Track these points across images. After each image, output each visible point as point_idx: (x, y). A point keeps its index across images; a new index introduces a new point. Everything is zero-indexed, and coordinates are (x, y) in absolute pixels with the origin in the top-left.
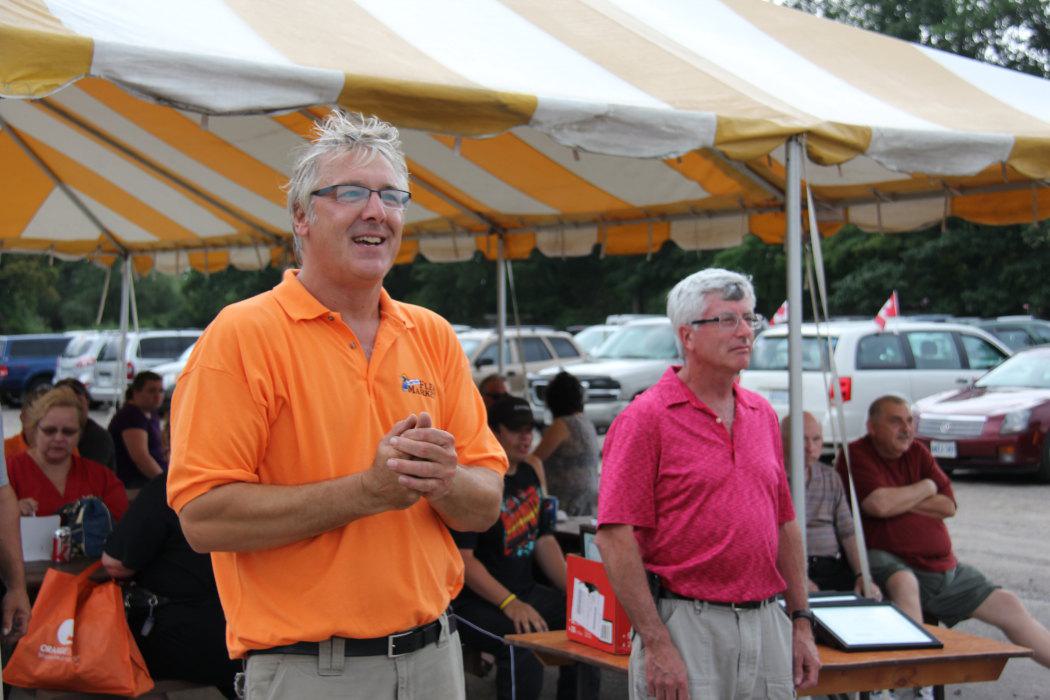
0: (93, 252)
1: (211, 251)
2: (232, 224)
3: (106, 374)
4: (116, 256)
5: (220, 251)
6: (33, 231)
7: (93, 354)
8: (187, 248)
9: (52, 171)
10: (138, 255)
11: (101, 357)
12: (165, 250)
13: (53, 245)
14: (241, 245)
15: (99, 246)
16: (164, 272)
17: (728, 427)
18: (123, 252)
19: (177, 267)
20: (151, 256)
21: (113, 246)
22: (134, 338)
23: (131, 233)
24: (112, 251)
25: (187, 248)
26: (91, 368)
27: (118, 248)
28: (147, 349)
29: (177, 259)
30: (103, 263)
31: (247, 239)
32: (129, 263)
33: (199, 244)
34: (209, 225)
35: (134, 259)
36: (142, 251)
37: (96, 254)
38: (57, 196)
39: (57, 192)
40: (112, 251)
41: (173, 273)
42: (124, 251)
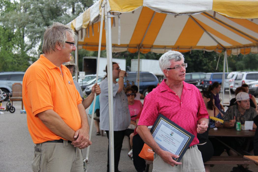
0: (216, 49)
1: (246, 48)
2: (249, 40)
3: (237, 84)
4: (222, 50)
5: (248, 48)
6: (199, 44)
7: (234, 78)
8: (240, 47)
9: (203, 28)
10: (228, 50)
11: (236, 79)
12: (234, 48)
13: (205, 47)
14: (254, 46)
15: (217, 47)
16: (234, 55)
17: (179, 97)
18: (224, 49)
19: (237, 53)
20: (230, 50)
21: (221, 47)
22: (245, 73)
23: (226, 44)
24: (221, 49)
25: (240, 47)
26: (233, 82)
27: (223, 48)
28: (249, 77)
29: (237, 51)
30: (218, 52)
31: (255, 45)
32: (226, 52)
33: (243, 46)
34: (244, 41)
35: (227, 51)
36: (229, 49)
37: (216, 50)
38: (205, 34)
39: (205, 33)
40: (221, 49)
41: (236, 54)
42: (224, 49)
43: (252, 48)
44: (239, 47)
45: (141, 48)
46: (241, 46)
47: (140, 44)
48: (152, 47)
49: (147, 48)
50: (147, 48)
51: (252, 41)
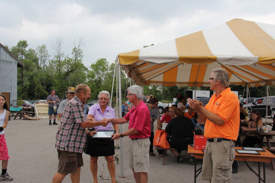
8: (254, 83)
9: (232, 72)
14: (261, 82)
21: (245, 83)
25: (254, 83)
30: (243, 85)
39: (233, 75)
42: (247, 84)
43: (260, 83)
44: (253, 82)
45: (196, 84)
46: (254, 82)
47: (195, 82)
48: (203, 83)
49: (200, 84)
50: (200, 84)
51: (258, 79)
